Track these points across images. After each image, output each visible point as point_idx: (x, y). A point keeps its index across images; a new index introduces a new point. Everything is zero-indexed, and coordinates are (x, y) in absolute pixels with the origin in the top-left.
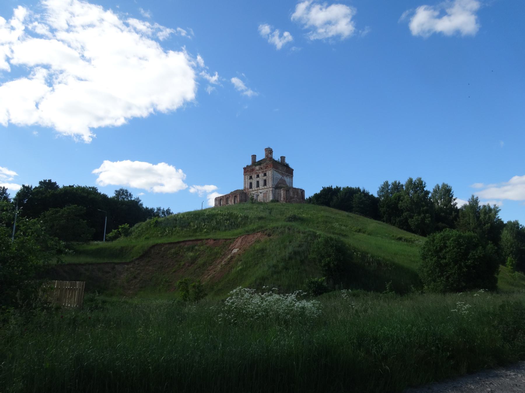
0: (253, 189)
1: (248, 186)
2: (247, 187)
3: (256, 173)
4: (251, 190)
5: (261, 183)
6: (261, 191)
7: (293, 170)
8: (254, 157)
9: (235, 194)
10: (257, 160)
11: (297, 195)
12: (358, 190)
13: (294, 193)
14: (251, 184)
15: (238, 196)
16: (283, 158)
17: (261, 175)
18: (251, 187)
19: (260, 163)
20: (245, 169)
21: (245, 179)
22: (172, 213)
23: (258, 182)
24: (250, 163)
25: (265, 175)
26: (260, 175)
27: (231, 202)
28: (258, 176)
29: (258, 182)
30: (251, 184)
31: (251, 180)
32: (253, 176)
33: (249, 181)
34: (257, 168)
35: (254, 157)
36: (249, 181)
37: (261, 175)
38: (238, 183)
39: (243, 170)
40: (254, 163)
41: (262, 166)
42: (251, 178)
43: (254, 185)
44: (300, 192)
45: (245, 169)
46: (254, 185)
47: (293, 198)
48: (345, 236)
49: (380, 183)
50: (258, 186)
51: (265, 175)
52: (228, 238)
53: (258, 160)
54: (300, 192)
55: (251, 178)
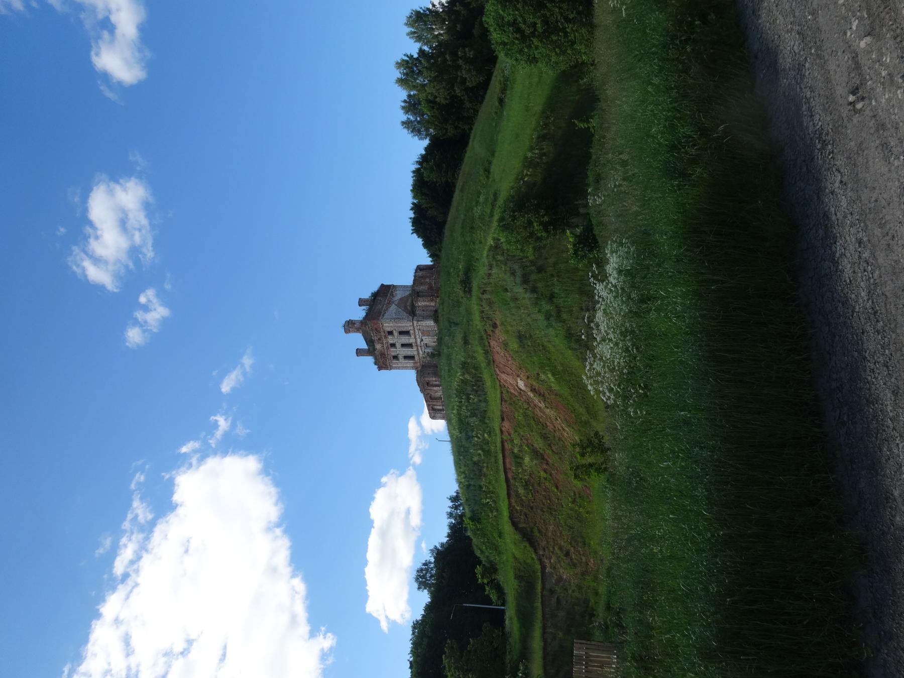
0: (415, 353)
1: (410, 363)
2: (412, 365)
4: (417, 358)
5: (405, 339)
6: (419, 341)
8: (359, 352)
9: (424, 386)
10: (366, 347)
12: (417, 172)
13: (422, 284)
14: (406, 357)
15: (427, 379)
16: (362, 302)
17: (391, 340)
19: (370, 342)
20: (380, 368)
21: (399, 368)
23: (403, 345)
24: (370, 360)
25: (391, 333)
26: (391, 342)
27: (438, 392)
28: (393, 345)
29: (403, 345)
30: (406, 357)
31: (400, 357)
32: (393, 354)
33: (401, 360)
34: (378, 346)
35: (359, 352)
36: (401, 360)
37: (391, 340)
38: (405, 379)
39: (383, 371)
40: (371, 351)
41: (376, 338)
42: (396, 357)
44: (420, 274)
45: (380, 368)
47: (430, 284)
48: (496, 195)
49: (406, 135)
50: (410, 345)
51: (391, 333)
52: (499, 396)
53: (364, 345)
54: (420, 274)
55: (396, 357)
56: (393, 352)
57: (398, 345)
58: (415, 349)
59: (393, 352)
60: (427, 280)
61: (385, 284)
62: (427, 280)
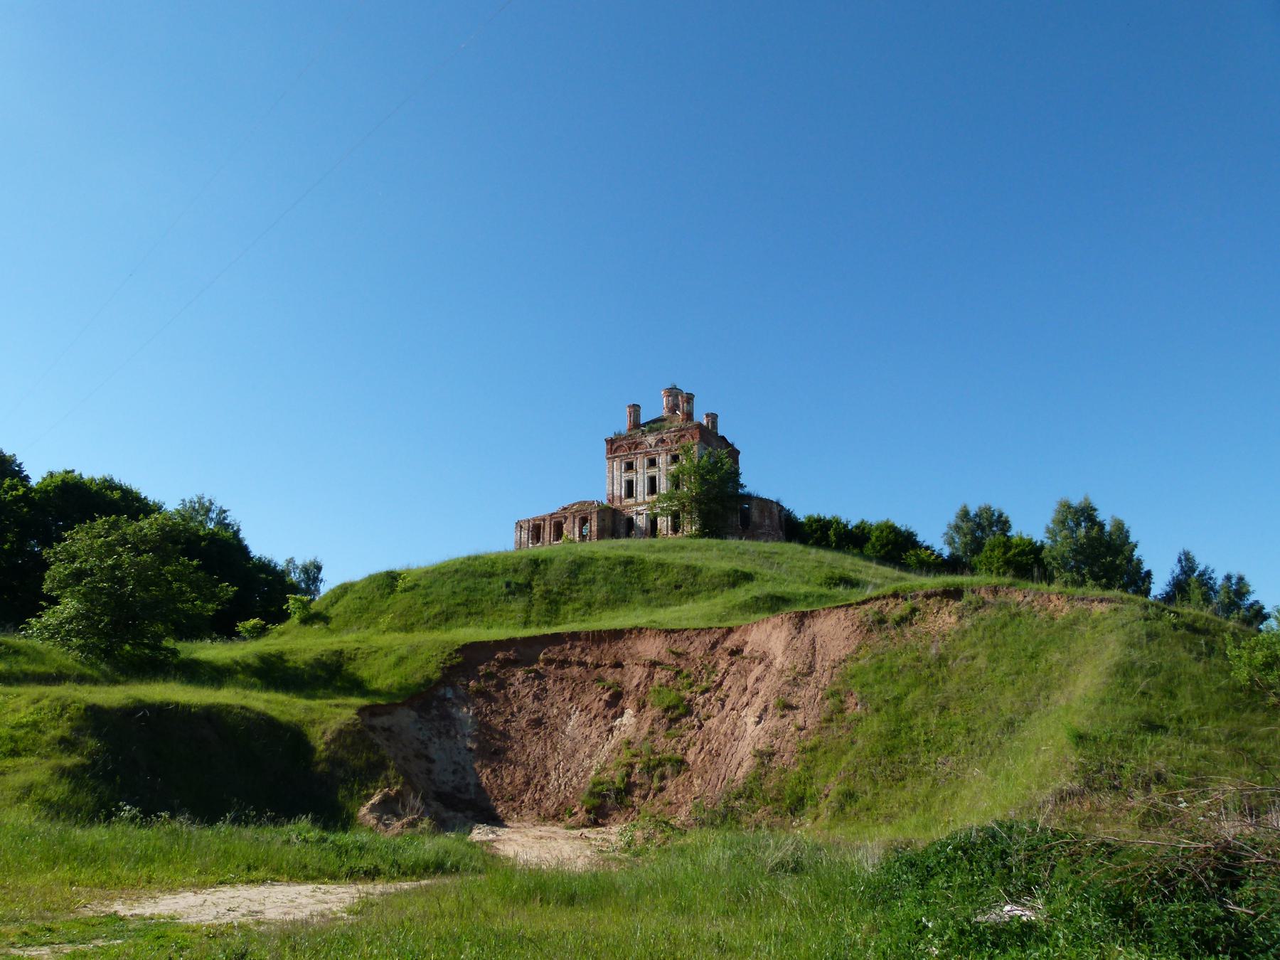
1: (620, 490)
2: (617, 493)
4: (631, 501)
7: (738, 453)
8: (635, 409)
10: (643, 420)
13: (762, 512)
14: (630, 484)
15: (594, 516)
16: (713, 417)
17: (662, 460)
18: (630, 492)
19: (656, 424)
20: (610, 442)
22: (742, 486)
23: (652, 480)
24: (623, 425)
28: (652, 463)
29: (652, 480)
30: (630, 484)
33: (626, 476)
34: (651, 439)
35: (635, 409)
37: (662, 460)
38: (599, 483)
39: (604, 446)
42: (630, 466)
43: (641, 487)
44: (775, 511)
45: (610, 442)
46: (641, 487)
47: (761, 526)
50: (653, 489)
52: (702, 625)
55: (630, 466)
56: (640, 462)
57: (653, 471)
59: (640, 462)
60: (767, 522)
62: (767, 522)
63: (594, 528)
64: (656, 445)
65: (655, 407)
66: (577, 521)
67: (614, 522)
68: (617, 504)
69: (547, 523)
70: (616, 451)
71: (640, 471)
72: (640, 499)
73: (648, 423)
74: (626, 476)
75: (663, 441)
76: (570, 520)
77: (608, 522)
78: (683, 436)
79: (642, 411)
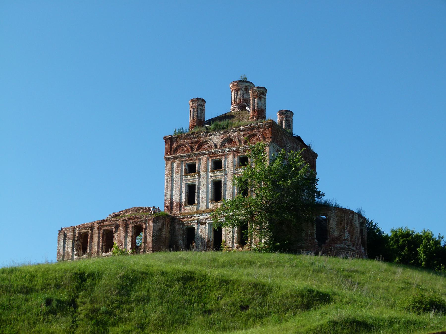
1: (180, 195)
2: (176, 199)
3: (211, 154)
4: (192, 208)
7: (315, 156)
8: (199, 103)
10: (208, 117)
11: (351, 232)
12: (429, 238)
13: (341, 224)
14: (191, 189)
15: (150, 225)
16: (287, 115)
17: (229, 162)
20: (170, 140)
23: (217, 185)
24: (184, 122)
28: (218, 165)
29: (217, 185)
30: (191, 189)
31: (192, 179)
33: (187, 180)
34: (216, 139)
35: (199, 103)
37: (229, 162)
42: (191, 169)
43: (204, 193)
44: (357, 223)
45: (170, 140)
46: (204, 193)
47: (340, 240)
49: (422, 230)
50: (217, 195)
55: (191, 169)
56: (204, 165)
57: (218, 175)
58: (212, 206)
59: (204, 165)
60: (347, 235)
61: (318, 161)
62: (347, 235)
63: (149, 239)
64: (222, 145)
65: (220, 103)
66: (130, 230)
67: (172, 232)
68: (176, 212)
69: (96, 232)
70: (176, 151)
71: (203, 174)
72: (202, 206)
73: (213, 120)
74: (187, 180)
75: (230, 141)
76: (122, 228)
77: (165, 233)
78: (253, 136)
79: (207, 107)
